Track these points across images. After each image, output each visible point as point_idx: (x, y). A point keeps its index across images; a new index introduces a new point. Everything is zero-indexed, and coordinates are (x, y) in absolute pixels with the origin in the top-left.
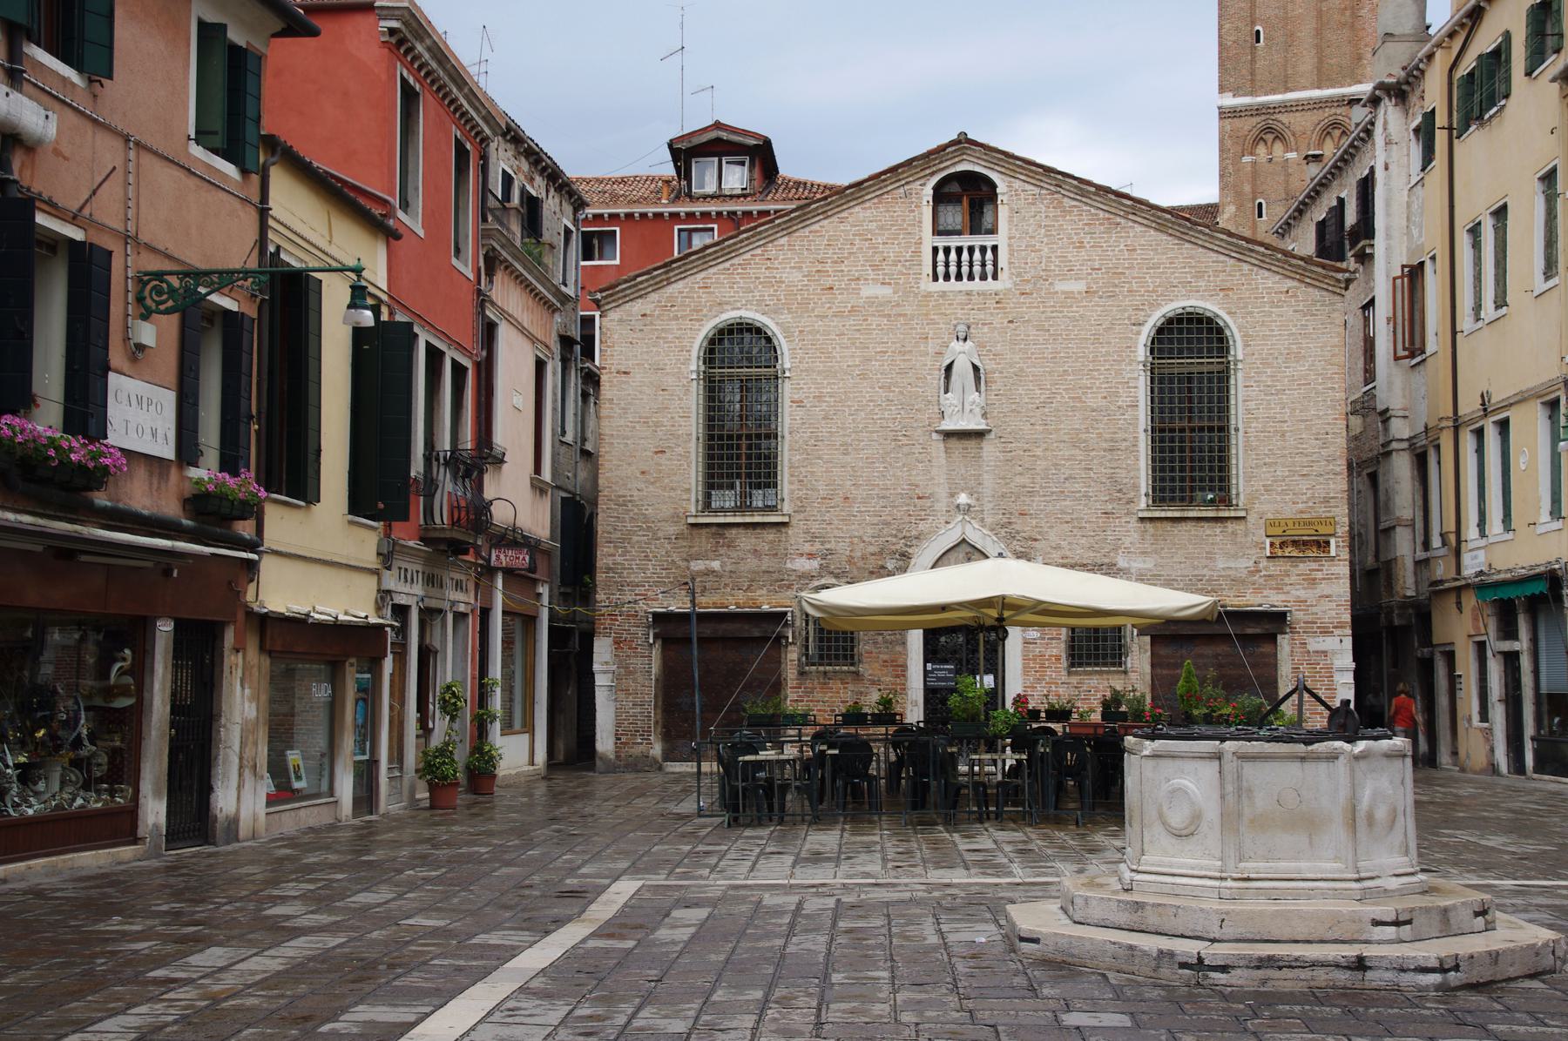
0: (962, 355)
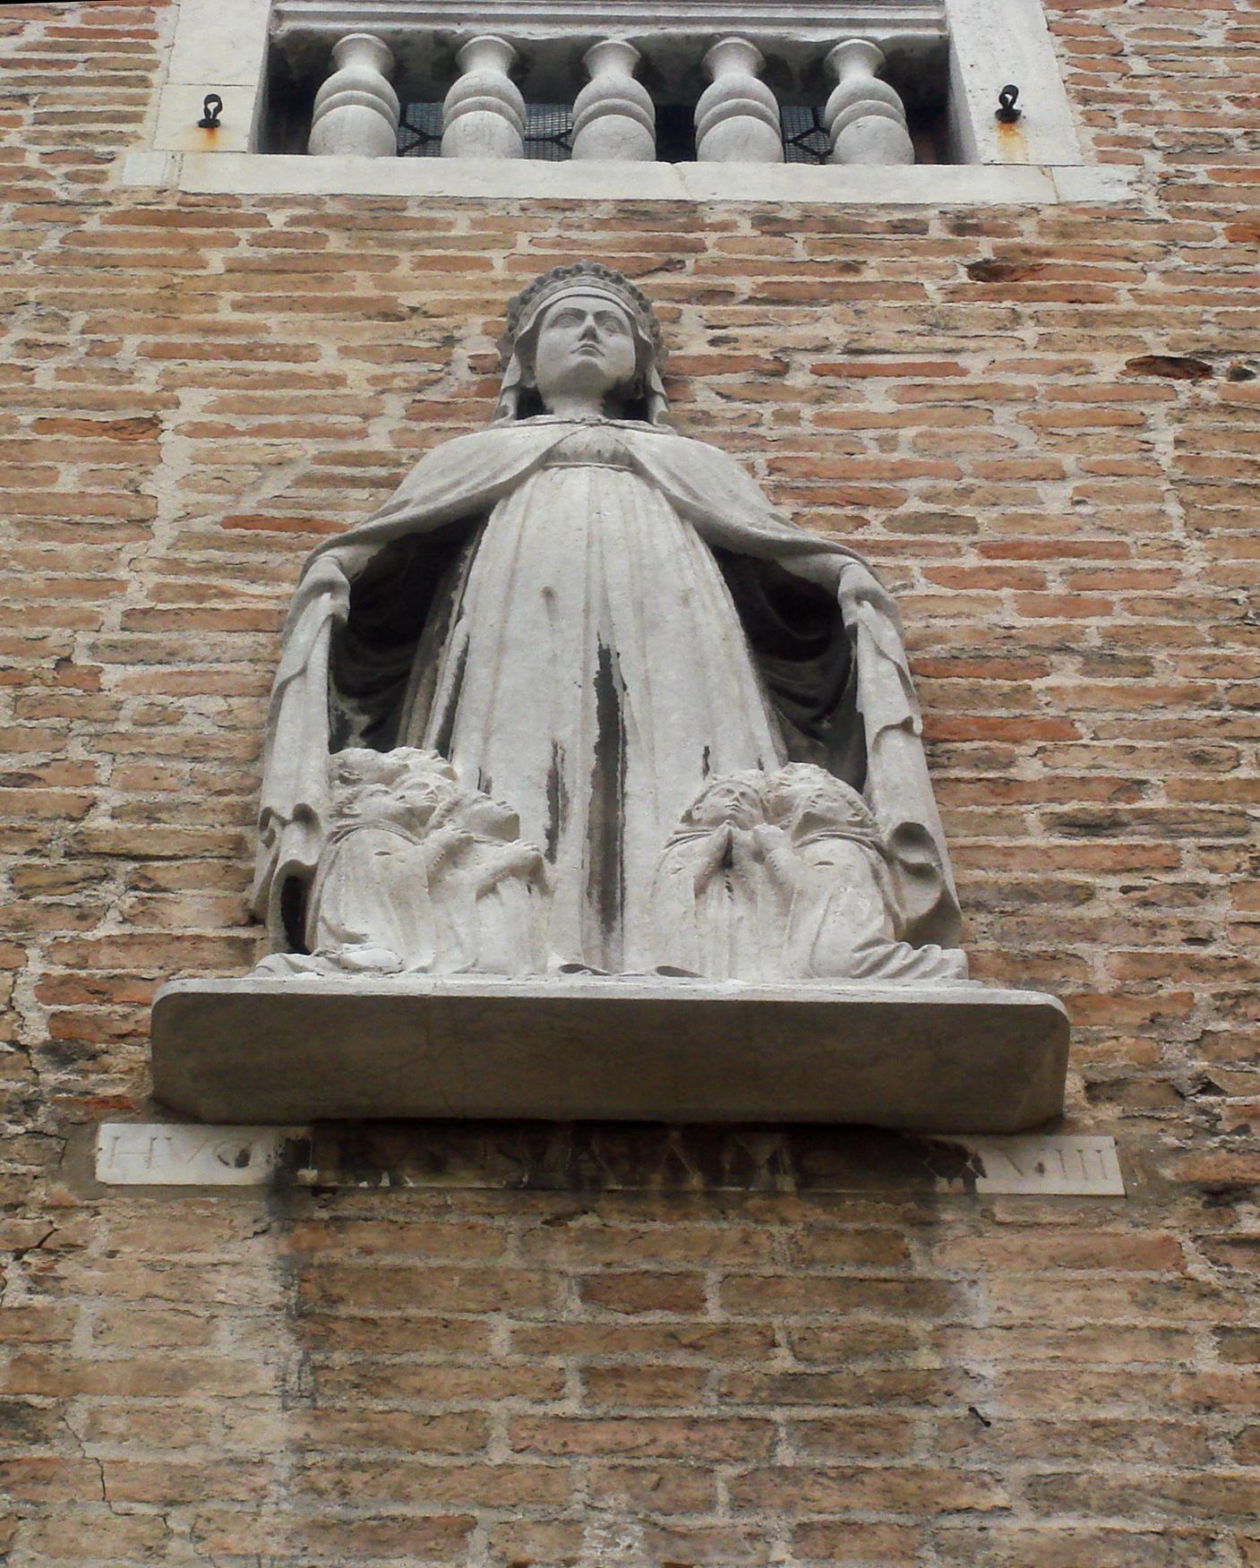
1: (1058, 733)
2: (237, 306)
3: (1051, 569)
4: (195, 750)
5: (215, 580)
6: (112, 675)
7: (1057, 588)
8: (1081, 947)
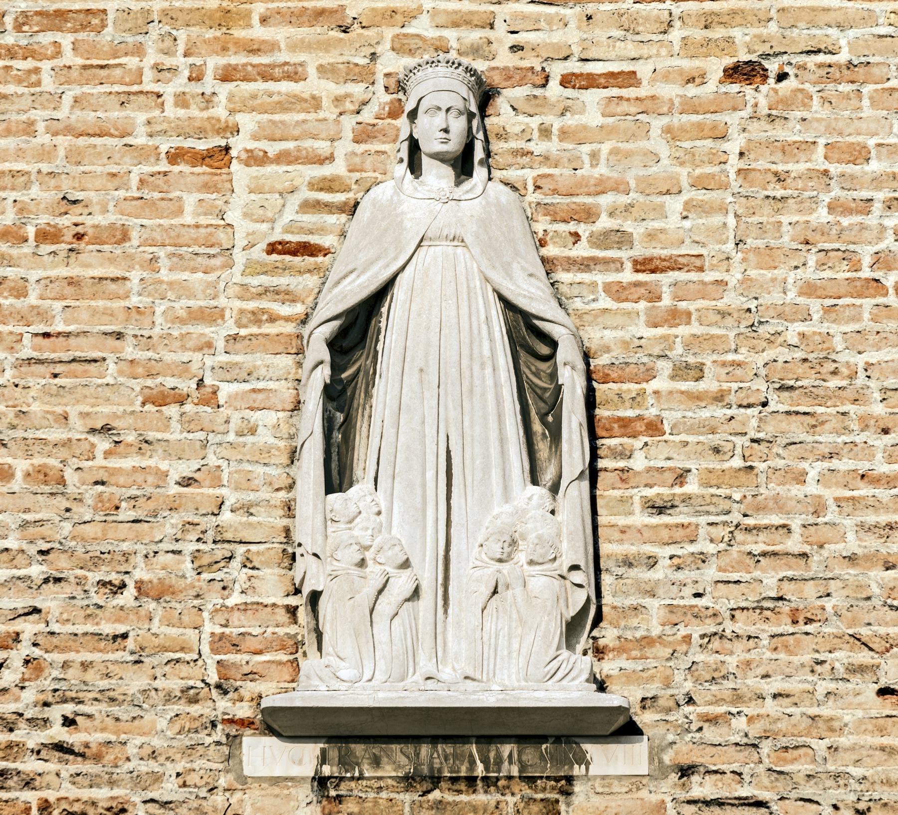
0: (445, 259)
1: (654, 427)
2: (264, 20)
3: (665, 279)
4: (262, 456)
5: (264, 304)
6: (226, 390)
7: (666, 301)
8: (647, 601)
